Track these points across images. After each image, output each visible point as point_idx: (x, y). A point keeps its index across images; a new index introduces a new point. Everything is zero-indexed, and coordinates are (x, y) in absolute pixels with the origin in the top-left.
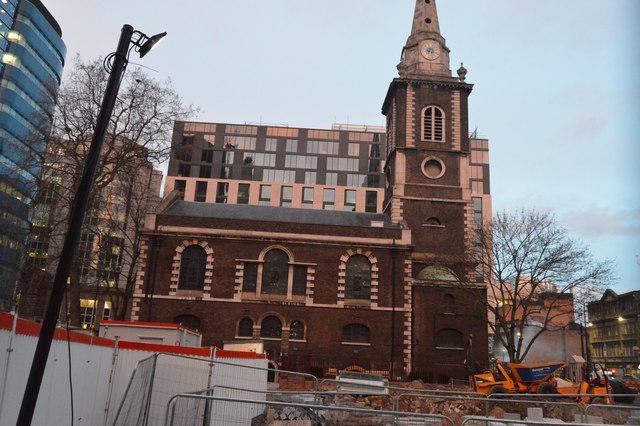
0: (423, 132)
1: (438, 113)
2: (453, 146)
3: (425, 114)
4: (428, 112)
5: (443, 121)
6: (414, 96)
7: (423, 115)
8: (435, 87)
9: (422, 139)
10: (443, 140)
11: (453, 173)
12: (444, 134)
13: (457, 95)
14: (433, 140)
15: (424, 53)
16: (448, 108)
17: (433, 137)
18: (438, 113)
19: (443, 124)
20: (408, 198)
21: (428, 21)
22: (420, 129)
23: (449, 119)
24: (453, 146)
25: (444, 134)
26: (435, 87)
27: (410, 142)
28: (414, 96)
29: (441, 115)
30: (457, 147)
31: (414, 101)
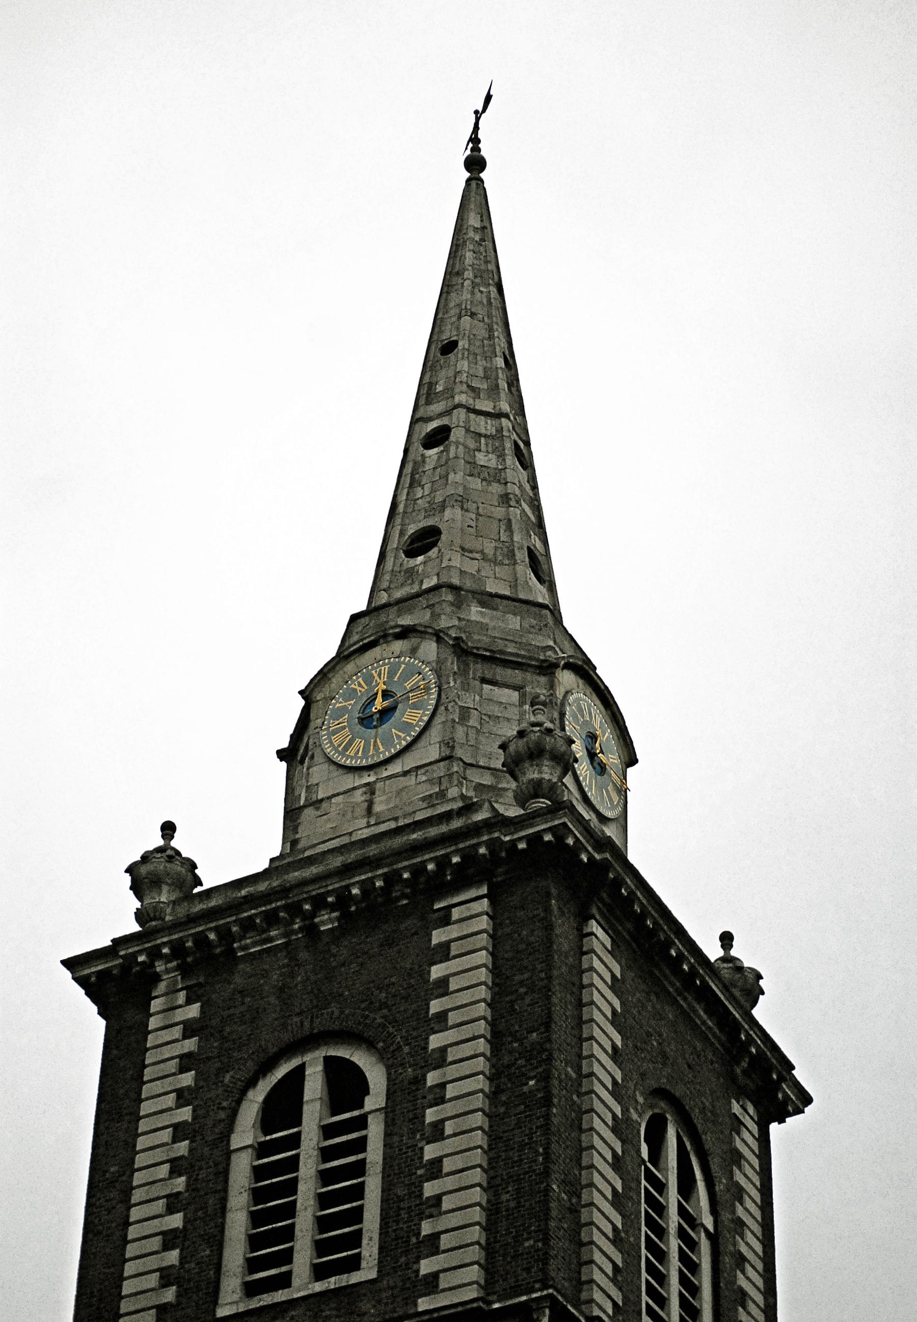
0: (235, 1253)
2: (431, 1284)
4: (283, 1108)
5: (375, 1131)
6: (190, 1029)
7: (246, 1132)
8: (327, 921)
14: (303, 1284)
16: (403, 1024)
18: (345, 1085)
19: (374, 1154)
21: (424, 541)
22: (218, 1242)
23: (408, 1098)
24: (431, 1284)
26: (327, 921)
28: (190, 1029)
31: (186, 1062)
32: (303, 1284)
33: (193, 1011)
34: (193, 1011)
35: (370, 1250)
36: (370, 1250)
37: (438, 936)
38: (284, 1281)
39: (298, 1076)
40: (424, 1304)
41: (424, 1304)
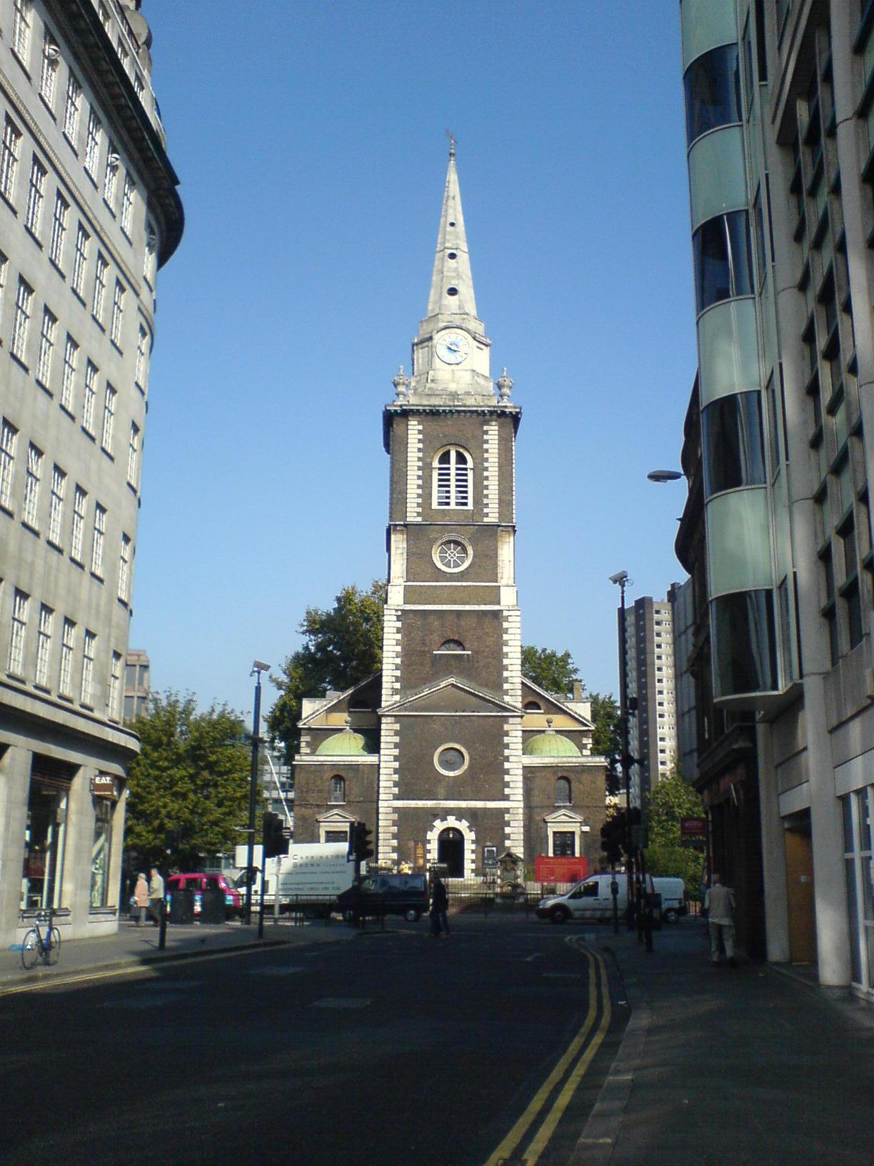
1: (461, 459)
2: (487, 515)
3: (440, 462)
4: (445, 459)
5: (470, 473)
6: (420, 432)
7: (436, 464)
9: (435, 506)
10: (470, 507)
11: (486, 565)
12: (470, 495)
13: (493, 432)
14: (453, 506)
15: (442, 351)
17: (453, 501)
18: (461, 459)
20: (408, 607)
23: (479, 470)
24: (487, 515)
25: (470, 495)
27: (413, 516)
28: (420, 432)
29: (465, 462)
30: (493, 518)
32: (453, 506)
33: (421, 427)
34: (421, 427)
35: (470, 501)
36: (470, 501)
37: (485, 428)
38: (448, 504)
39: (448, 453)
40: (485, 520)
41: (485, 520)
